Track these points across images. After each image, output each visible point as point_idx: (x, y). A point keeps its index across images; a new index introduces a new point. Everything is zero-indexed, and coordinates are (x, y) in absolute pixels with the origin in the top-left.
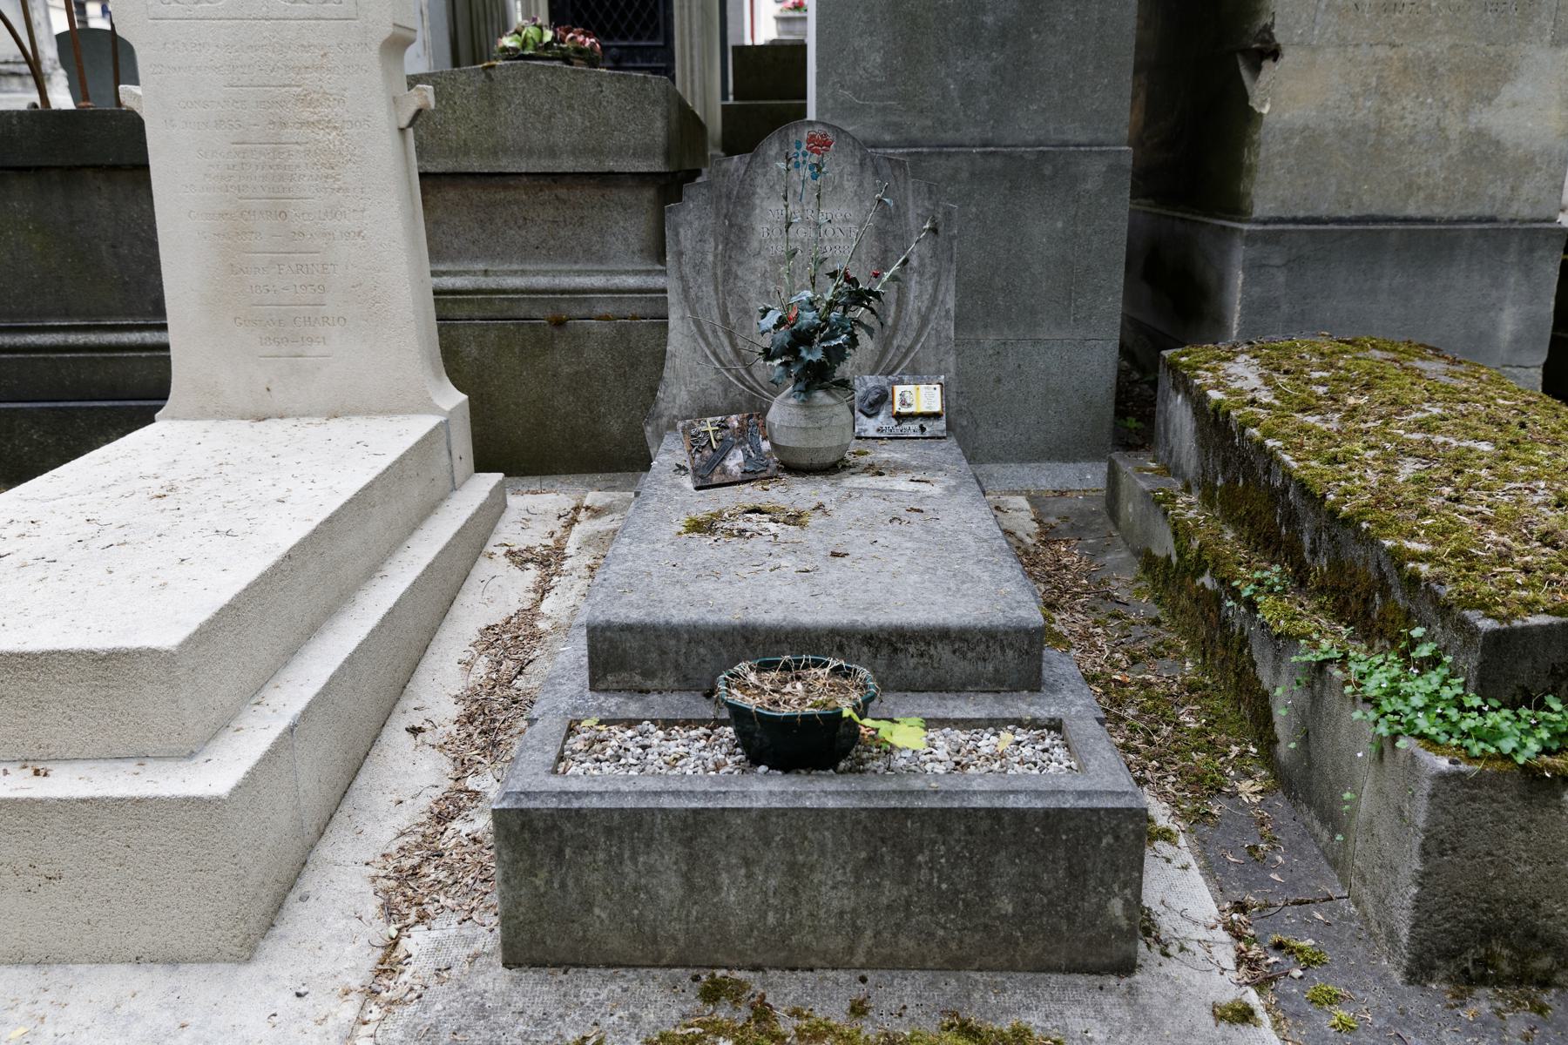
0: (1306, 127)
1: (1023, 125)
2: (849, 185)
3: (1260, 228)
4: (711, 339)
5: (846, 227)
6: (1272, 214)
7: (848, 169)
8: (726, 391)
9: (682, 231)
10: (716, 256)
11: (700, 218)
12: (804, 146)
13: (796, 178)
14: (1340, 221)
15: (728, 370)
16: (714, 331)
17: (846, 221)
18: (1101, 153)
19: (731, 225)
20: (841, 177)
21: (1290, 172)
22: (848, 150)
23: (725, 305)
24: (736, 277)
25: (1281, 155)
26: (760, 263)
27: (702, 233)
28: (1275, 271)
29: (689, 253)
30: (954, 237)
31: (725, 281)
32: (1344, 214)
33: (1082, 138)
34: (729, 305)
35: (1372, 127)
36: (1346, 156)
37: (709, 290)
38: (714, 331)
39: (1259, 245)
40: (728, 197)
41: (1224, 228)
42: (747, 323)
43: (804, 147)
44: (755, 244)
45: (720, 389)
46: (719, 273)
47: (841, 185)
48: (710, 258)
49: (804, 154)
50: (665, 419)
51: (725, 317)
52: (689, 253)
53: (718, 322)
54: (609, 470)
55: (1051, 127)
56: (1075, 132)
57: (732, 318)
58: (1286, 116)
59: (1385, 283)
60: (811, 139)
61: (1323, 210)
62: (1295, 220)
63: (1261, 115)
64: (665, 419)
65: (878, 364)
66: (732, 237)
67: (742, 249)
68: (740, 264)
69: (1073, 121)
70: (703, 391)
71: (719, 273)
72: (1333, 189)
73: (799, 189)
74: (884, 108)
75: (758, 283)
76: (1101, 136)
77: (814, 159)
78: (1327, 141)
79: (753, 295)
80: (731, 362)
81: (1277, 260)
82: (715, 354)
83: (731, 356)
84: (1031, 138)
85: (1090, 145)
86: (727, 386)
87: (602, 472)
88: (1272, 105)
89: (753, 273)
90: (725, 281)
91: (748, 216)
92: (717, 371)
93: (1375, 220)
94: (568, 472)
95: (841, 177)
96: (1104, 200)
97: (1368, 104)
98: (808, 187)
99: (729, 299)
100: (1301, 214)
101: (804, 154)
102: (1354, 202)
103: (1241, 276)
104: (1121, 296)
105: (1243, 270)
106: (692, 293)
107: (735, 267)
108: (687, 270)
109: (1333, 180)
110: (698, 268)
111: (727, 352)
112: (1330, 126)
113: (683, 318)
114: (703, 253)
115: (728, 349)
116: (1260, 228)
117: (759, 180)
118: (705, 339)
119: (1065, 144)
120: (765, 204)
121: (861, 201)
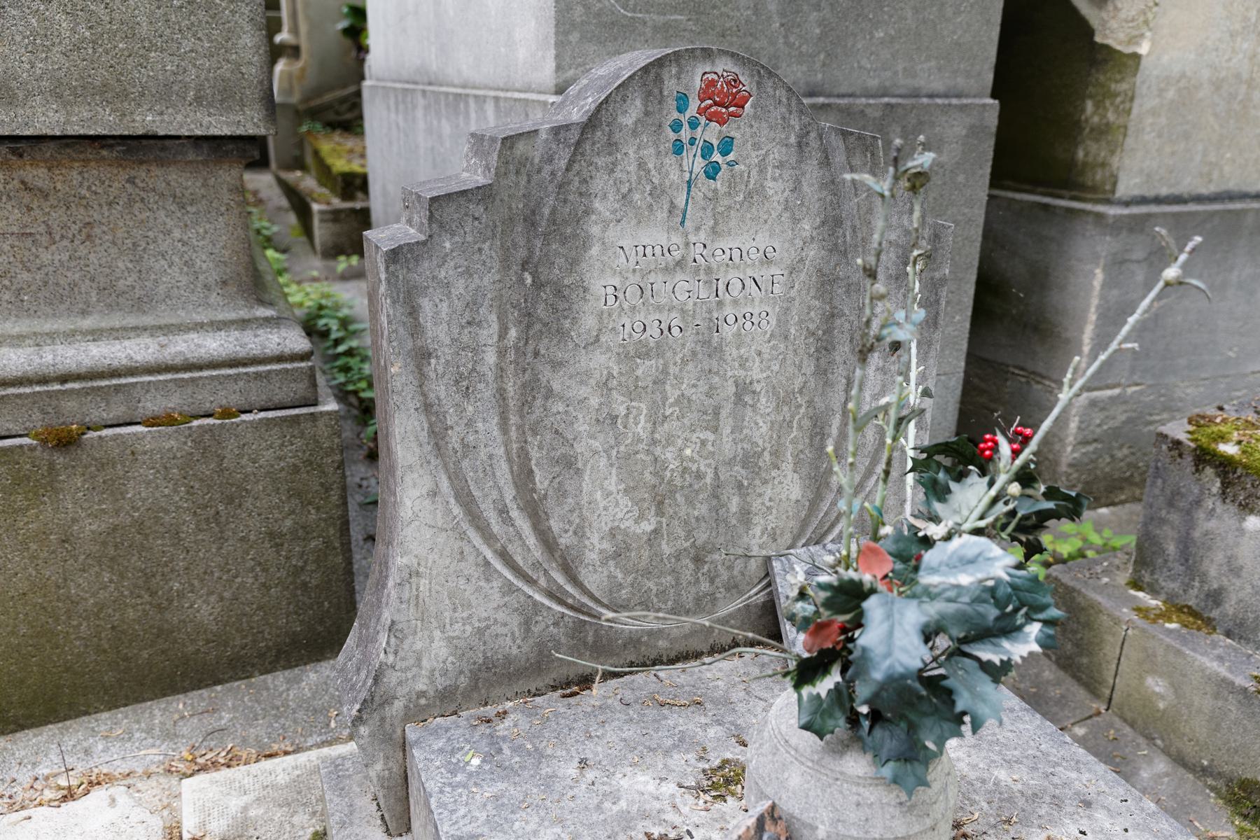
0: (1183, 75)
1: (864, 62)
2: (776, 189)
3: (1126, 211)
4: (496, 528)
5: (764, 274)
6: (1137, 192)
7: (776, 154)
8: (527, 624)
9: (426, 304)
10: (502, 353)
11: (468, 273)
12: (694, 105)
13: (674, 176)
14: (1199, 199)
15: (531, 581)
16: (503, 512)
17: (766, 260)
18: (962, 108)
19: (538, 285)
20: (762, 171)
21: (1160, 136)
22: (777, 113)
23: (524, 455)
24: (549, 393)
25: (1154, 112)
26: (600, 362)
27: (473, 305)
28: (1134, 267)
29: (446, 353)
30: (943, 281)
31: (525, 405)
32: (1204, 191)
33: (938, 86)
34: (534, 454)
35: (1245, 76)
36: (1216, 115)
37: (489, 426)
38: (503, 512)
39: (1124, 233)
40: (531, 221)
41: (1046, 207)
42: (569, 486)
43: (692, 110)
44: (589, 322)
45: (515, 622)
46: (511, 388)
47: (760, 190)
48: (491, 357)
49: (693, 125)
50: (398, 705)
51: (523, 478)
52: (446, 353)
53: (509, 493)
54: (199, 684)
55: (900, 67)
56: (930, 77)
57: (541, 480)
58: (1165, 59)
59: (1234, 277)
60: (708, 90)
61: (1188, 185)
62: (1158, 200)
63: (1136, 57)
64: (398, 705)
65: (804, 524)
66: (541, 311)
67: (562, 335)
68: (556, 365)
69: (928, 59)
70: (480, 632)
71: (511, 388)
72: (1198, 158)
73: (680, 200)
74: (667, 26)
75: (594, 402)
76: (961, 81)
77: (712, 133)
78: (1201, 95)
79: (582, 427)
80: (537, 565)
81: (1139, 254)
82: (504, 556)
83: (538, 553)
84: (873, 83)
85: (946, 96)
86: (530, 613)
87: (185, 691)
88: (1154, 42)
89: (584, 380)
90: (525, 405)
91: (574, 263)
92: (509, 589)
93: (1230, 196)
94: (112, 705)
95: (762, 171)
96: (961, 178)
97: (1245, 46)
98: (697, 194)
99: (534, 441)
100: (1164, 191)
101: (693, 125)
102: (1215, 175)
103: (1099, 275)
104: (969, 313)
105: (1104, 270)
106: (454, 439)
107: (546, 374)
108: (441, 390)
109: (1200, 147)
110: (465, 385)
111: (529, 548)
112: (1206, 74)
113: (434, 494)
114: (476, 350)
115: (531, 540)
116: (1126, 211)
117: (600, 182)
118: (489, 537)
119: (915, 94)
120: (611, 234)
121: (796, 221)
